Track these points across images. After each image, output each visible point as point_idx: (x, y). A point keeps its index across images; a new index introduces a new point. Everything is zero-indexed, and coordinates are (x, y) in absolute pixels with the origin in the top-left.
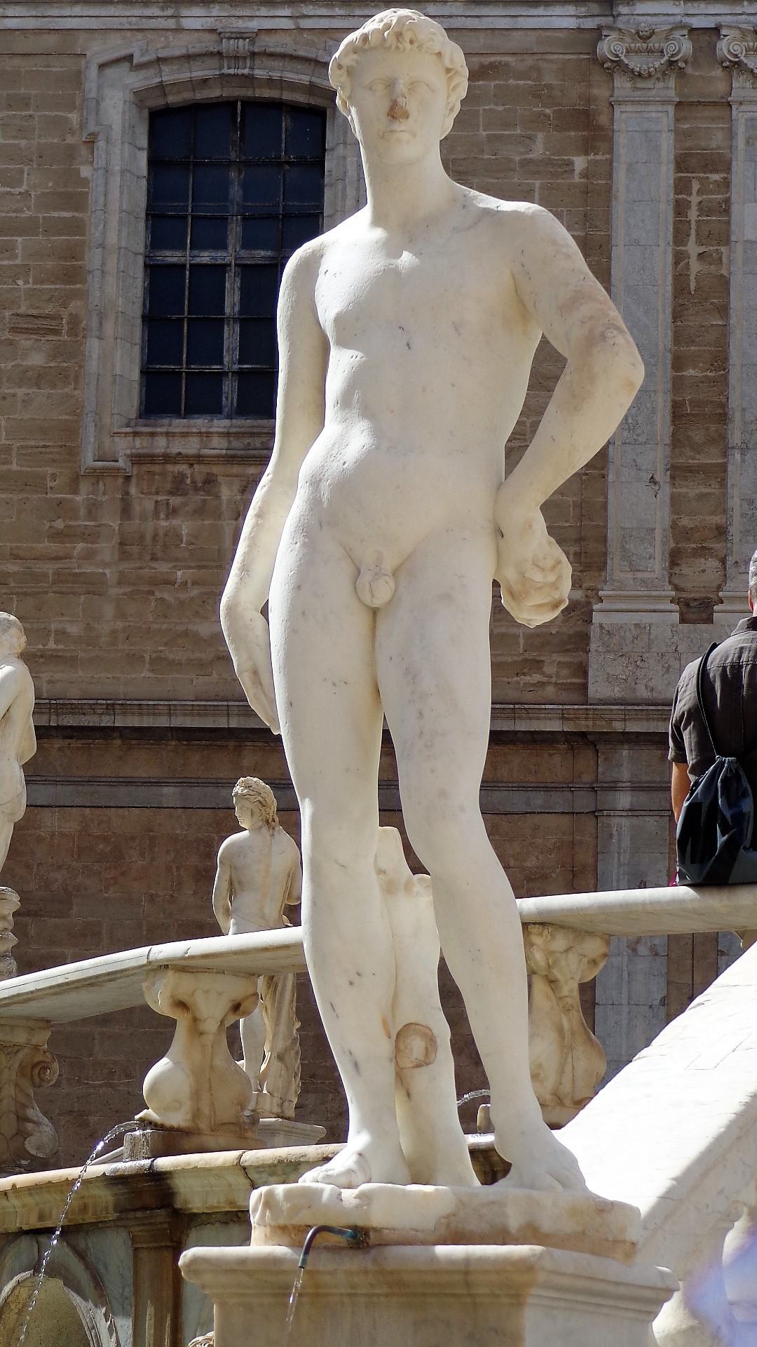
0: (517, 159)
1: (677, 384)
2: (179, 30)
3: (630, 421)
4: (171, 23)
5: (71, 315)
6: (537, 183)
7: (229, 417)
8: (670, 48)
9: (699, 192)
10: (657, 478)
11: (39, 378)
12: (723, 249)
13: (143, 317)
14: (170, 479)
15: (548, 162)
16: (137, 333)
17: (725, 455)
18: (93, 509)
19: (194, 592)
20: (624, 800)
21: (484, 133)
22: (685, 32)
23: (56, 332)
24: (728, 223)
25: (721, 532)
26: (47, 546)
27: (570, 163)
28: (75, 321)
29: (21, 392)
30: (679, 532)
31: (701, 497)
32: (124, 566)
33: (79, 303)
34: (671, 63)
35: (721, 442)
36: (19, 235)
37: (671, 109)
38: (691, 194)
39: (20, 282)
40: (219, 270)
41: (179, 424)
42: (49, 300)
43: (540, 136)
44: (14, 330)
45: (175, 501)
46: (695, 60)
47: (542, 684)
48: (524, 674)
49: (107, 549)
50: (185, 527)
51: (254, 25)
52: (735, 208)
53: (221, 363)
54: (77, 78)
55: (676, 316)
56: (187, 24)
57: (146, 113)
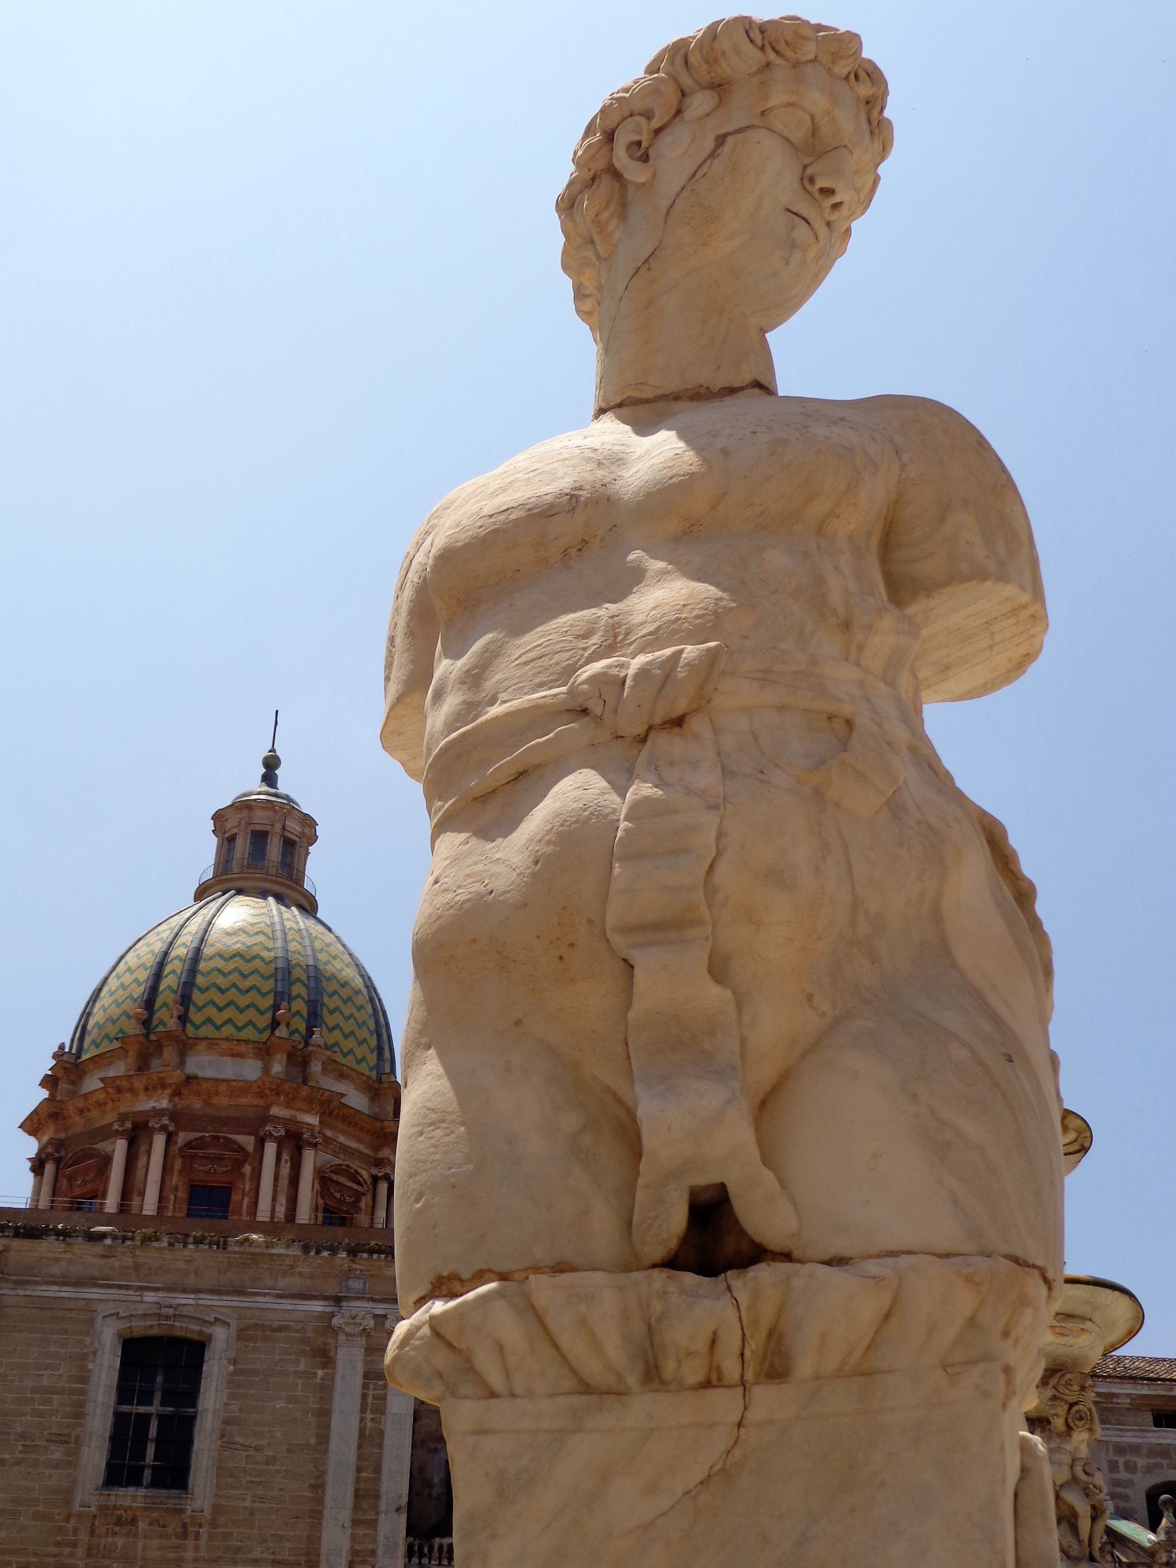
0: (292, 1370)
1: (358, 1480)
2: (141, 1302)
4: (138, 1299)
5: (77, 1435)
7: (145, 1488)
8: (365, 1323)
9: (374, 1389)
10: (345, 1525)
11: (57, 1465)
12: (383, 1417)
13: (110, 1438)
16: (106, 1444)
17: (377, 1514)
18: (76, 1531)
21: (277, 1357)
22: (371, 1315)
23: (68, 1442)
24: (385, 1405)
25: (373, 1553)
26: (55, 1550)
27: (316, 1373)
28: (78, 1438)
29: (47, 1471)
30: (354, 1553)
31: (365, 1535)
33: (81, 1429)
34: (364, 1330)
35: (375, 1508)
36: (56, 1394)
37: (363, 1350)
39: (54, 1418)
40: (148, 1416)
41: (121, 1491)
42: (67, 1427)
43: (303, 1360)
44: (48, 1441)
45: (116, 1529)
46: (375, 1329)
49: (80, 1551)
50: (120, 1542)
51: (177, 1301)
52: (388, 1398)
53: (144, 1461)
54: (91, 1322)
55: (359, 1447)
56: (146, 1299)
57: (122, 1340)
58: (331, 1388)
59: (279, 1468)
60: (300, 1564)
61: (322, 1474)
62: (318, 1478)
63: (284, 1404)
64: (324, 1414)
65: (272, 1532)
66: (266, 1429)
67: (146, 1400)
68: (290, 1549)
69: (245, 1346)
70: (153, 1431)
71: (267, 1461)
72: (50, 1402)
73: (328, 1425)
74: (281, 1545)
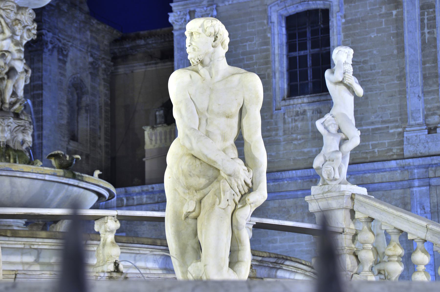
0: (378, 14)
1: (424, 69)
3: (412, 81)
6: (384, 20)
9: (427, 15)
12: (435, 30)
14: (294, 112)
15: (386, 14)
19: (303, 141)
20: (416, 183)
21: (368, 9)
24: (435, 22)
27: (392, 13)
28: (269, 75)
31: (432, 99)
32: (285, 136)
38: (424, 16)
40: (306, 56)
43: (384, 7)
45: (296, 118)
47: (393, 155)
48: (388, 153)
49: (281, 133)
50: (299, 124)
55: (423, 50)
58: (402, 20)
59: (378, 71)
60: (397, 121)
61: (403, 69)
62: (400, 72)
63: (376, 35)
64: (400, 35)
65: (379, 106)
66: (368, 50)
67: (303, 47)
68: (391, 114)
69: (350, 6)
70: (309, 63)
71: (371, 68)
72: (251, 59)
73: (403, 41)
74: (386, 112)
